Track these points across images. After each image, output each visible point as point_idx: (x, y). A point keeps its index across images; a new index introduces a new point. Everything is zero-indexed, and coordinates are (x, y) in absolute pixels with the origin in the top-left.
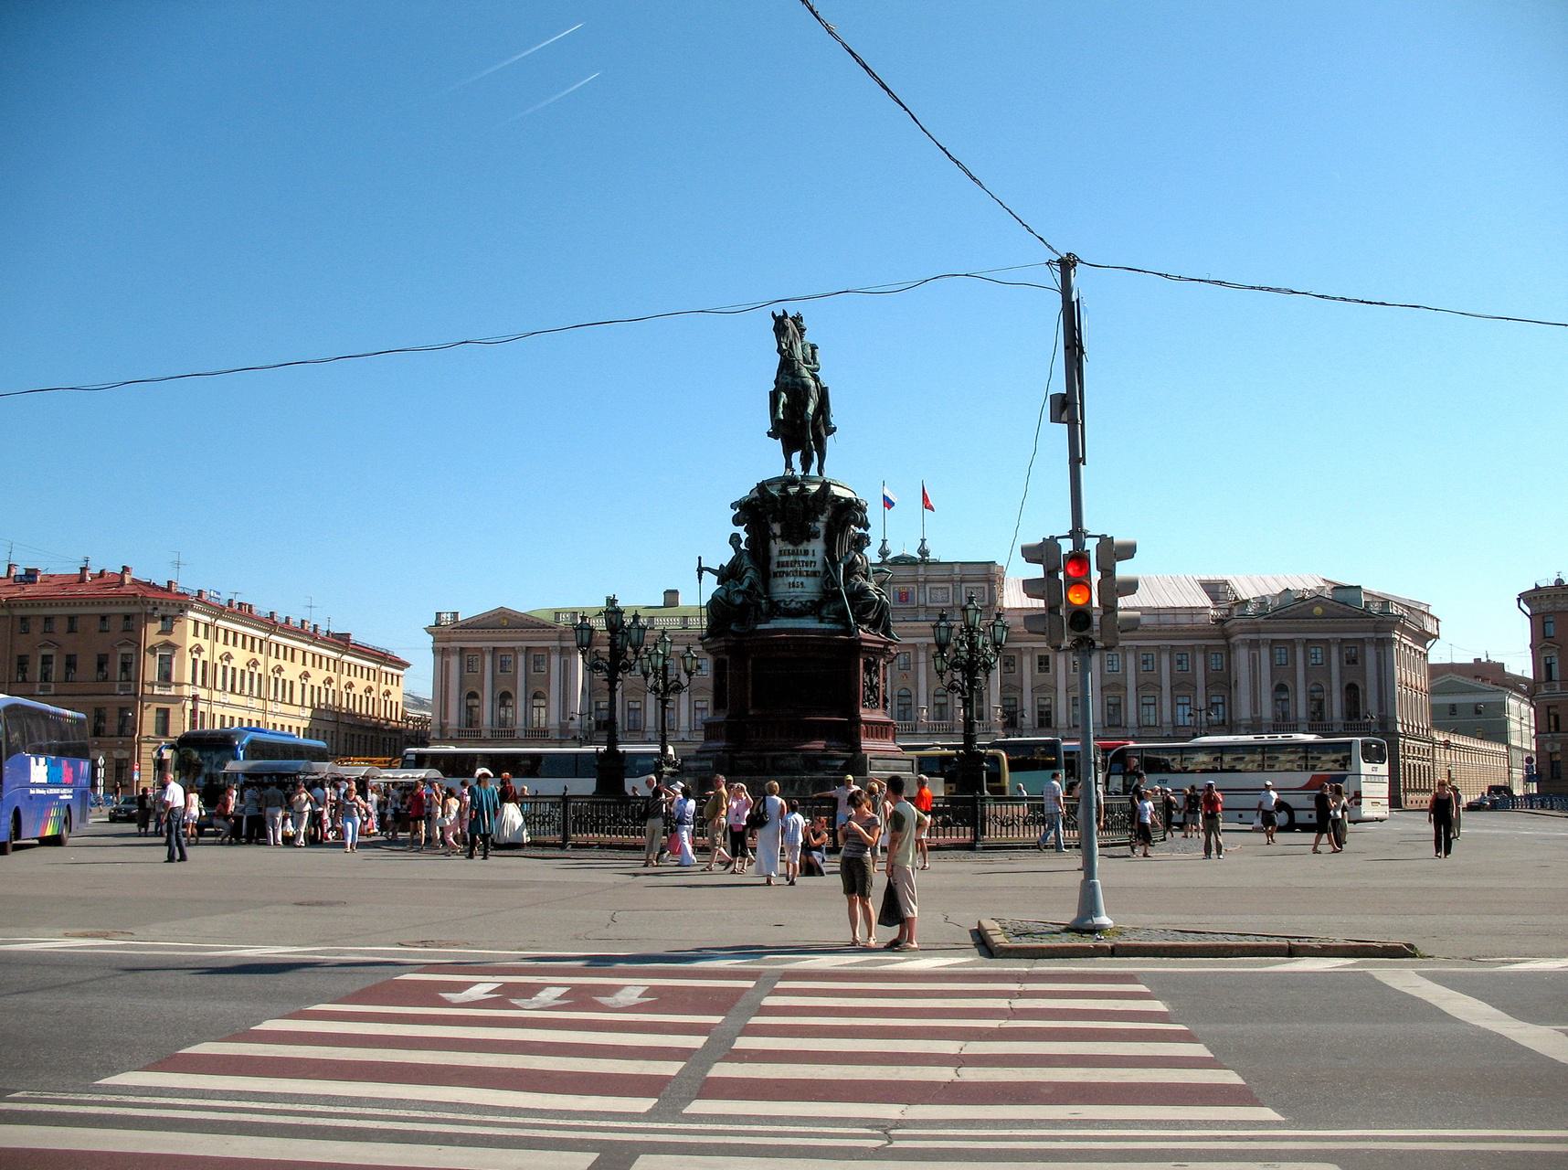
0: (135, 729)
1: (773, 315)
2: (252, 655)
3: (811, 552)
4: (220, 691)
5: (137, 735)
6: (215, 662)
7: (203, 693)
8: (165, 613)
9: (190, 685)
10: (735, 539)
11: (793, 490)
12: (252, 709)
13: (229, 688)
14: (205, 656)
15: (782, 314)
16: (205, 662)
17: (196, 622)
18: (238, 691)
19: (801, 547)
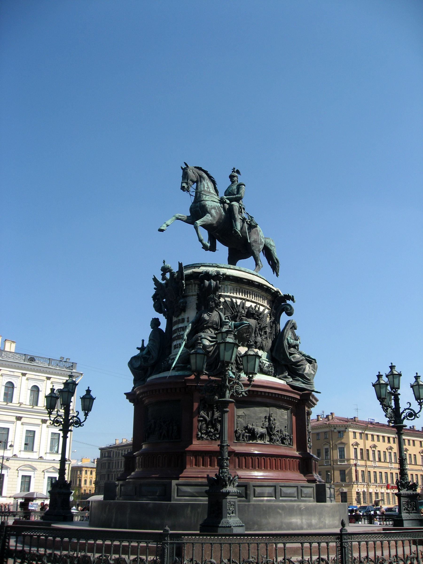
0: (331, 479)
1: (182, 168)
2: (389, 445)
3: (186, 320)
4: (372, 461)
5: (332, 482)
6: (367, 448)
7: (360, 463)
8: (339, 430)
9: (353, 459)
10: (155, 323)
11: (168, 275)
12: (391, 468)
13: (377, 459)
14: (361, 446)
15: (186, 166)
16: (361, 449)
17: (354, 433)
18: (382, 460)
19: (180, 318)
